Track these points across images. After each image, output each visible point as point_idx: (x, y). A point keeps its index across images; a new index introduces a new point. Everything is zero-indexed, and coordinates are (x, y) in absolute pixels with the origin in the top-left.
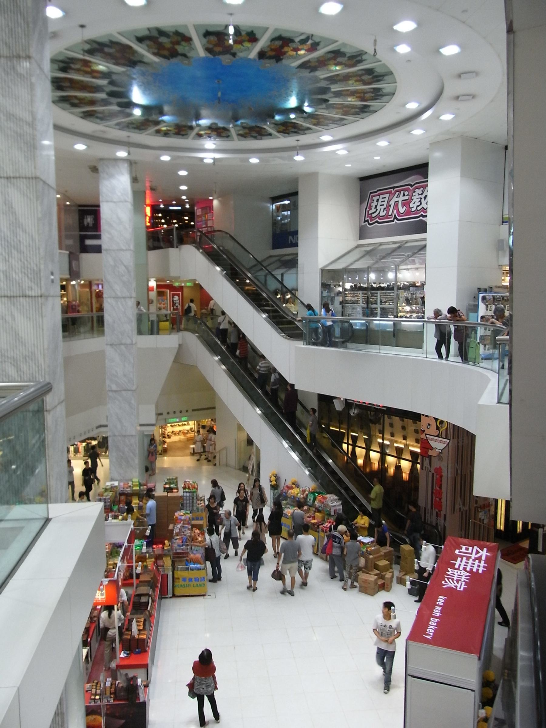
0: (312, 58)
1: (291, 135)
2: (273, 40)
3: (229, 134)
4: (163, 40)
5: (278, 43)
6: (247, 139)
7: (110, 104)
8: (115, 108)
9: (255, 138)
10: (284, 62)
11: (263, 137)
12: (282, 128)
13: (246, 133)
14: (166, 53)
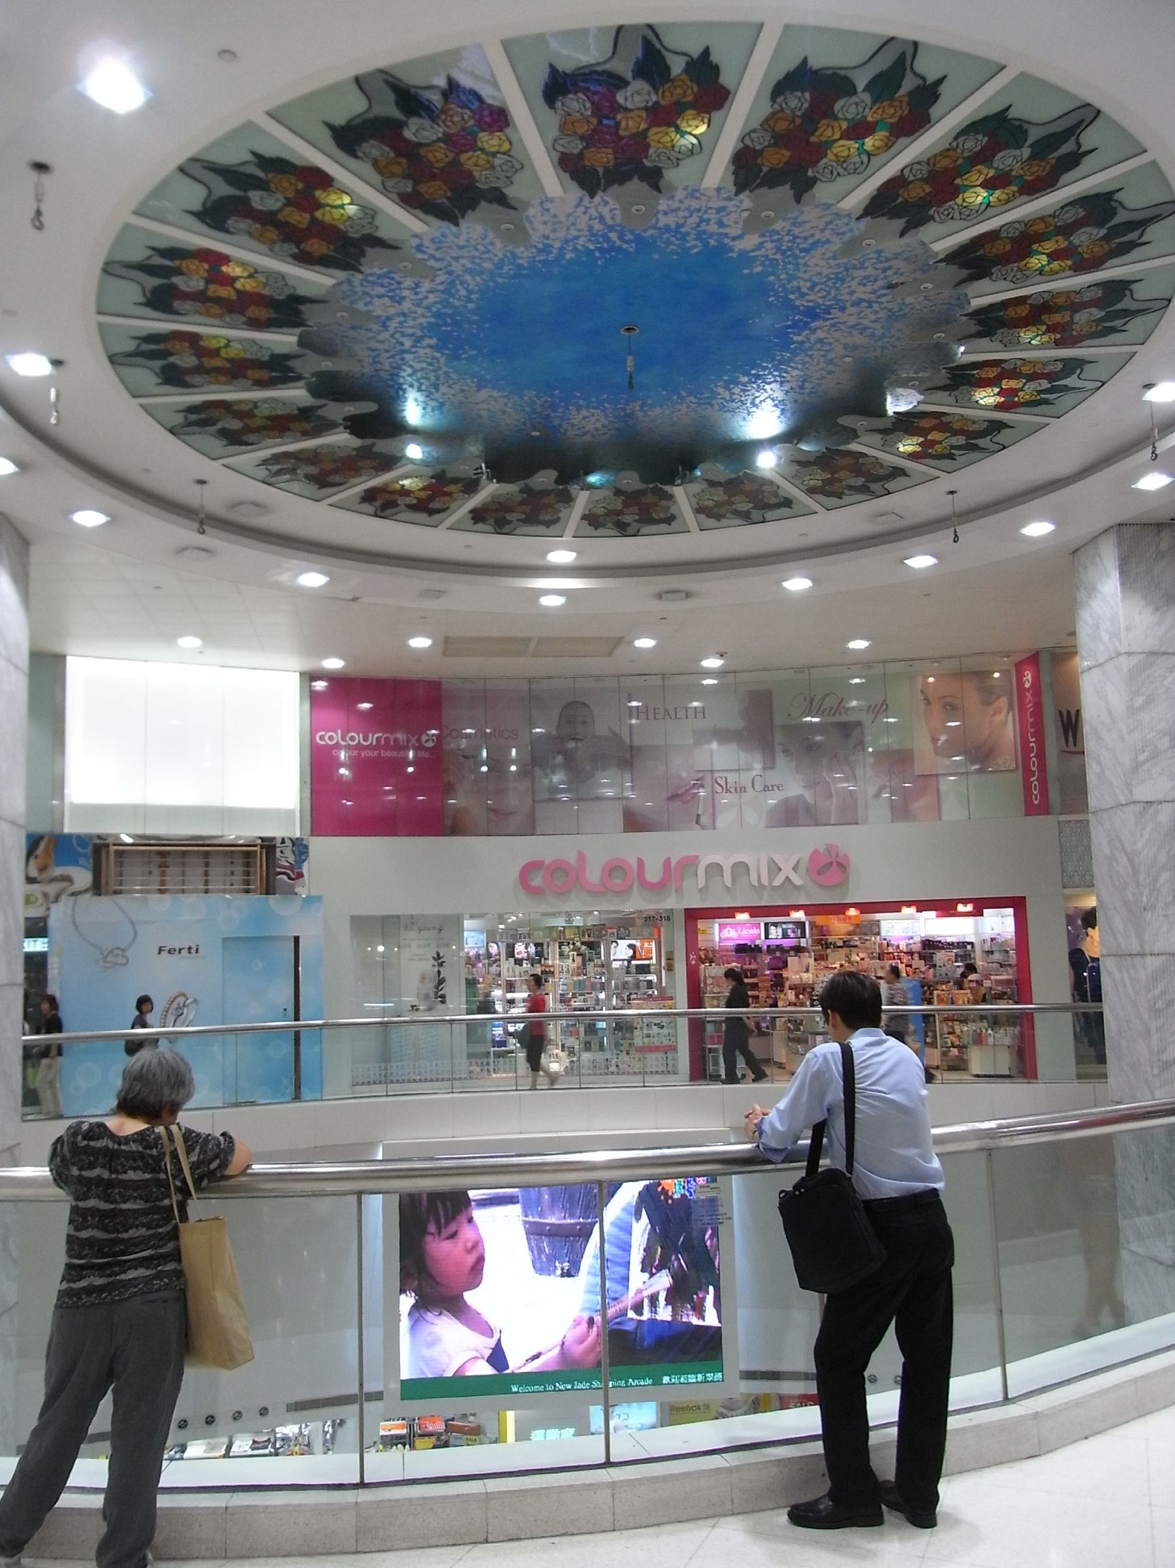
0: (911, 165)
1: (846, 499)
2: (782, 88)
3: (673, 510)
4: (417, 130)
5: (798, 102)
6: (724, 522)
7: (324, 426)
8: (341, 439)
9: (746, 518)
10: (823, 191)
11: (769, 515)
12: (818, 477)
13: (719, 504)
14: (437, 192)
